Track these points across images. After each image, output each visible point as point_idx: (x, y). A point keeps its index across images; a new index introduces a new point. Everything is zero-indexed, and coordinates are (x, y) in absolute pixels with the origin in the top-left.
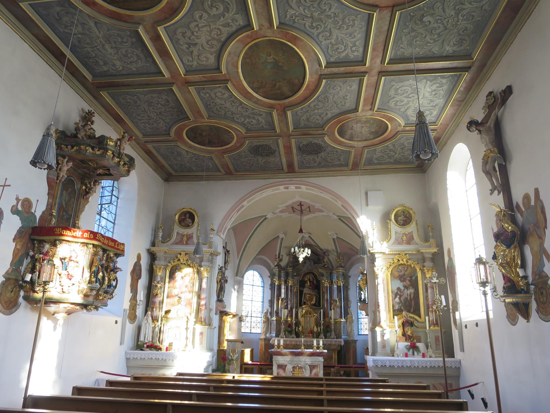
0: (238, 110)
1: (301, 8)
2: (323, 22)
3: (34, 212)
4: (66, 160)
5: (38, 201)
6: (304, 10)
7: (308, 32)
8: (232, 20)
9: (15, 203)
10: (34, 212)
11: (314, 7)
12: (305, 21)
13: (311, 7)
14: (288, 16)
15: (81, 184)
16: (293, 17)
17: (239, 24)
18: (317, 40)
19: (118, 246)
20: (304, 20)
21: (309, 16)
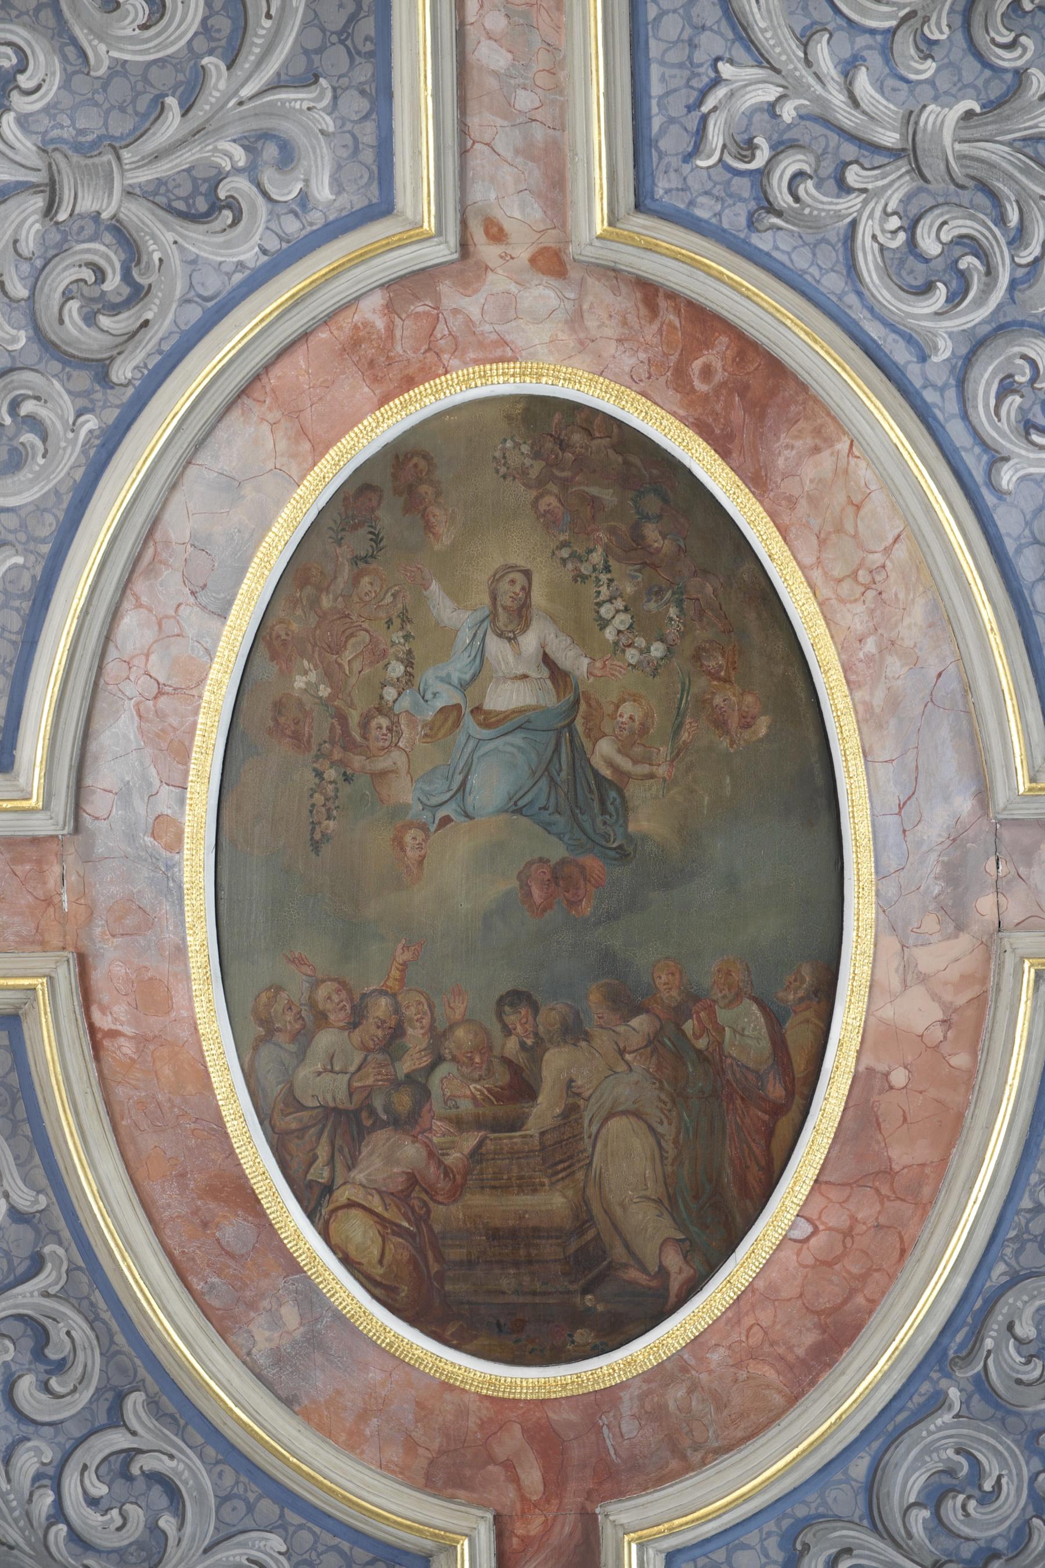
0: (59, 1513)
1: (822, 51)
2: (1001, 220)
6: (848, 68)
7: (874, 330)
8: (251, 144)
11: (927, 48)
12: (854, 201)
13: (905, 46)
14: (715, 136)
16: (751, 147)
17: (304, 199)
18: (957, 432)
20: (843, 188)
21: (890, 138)
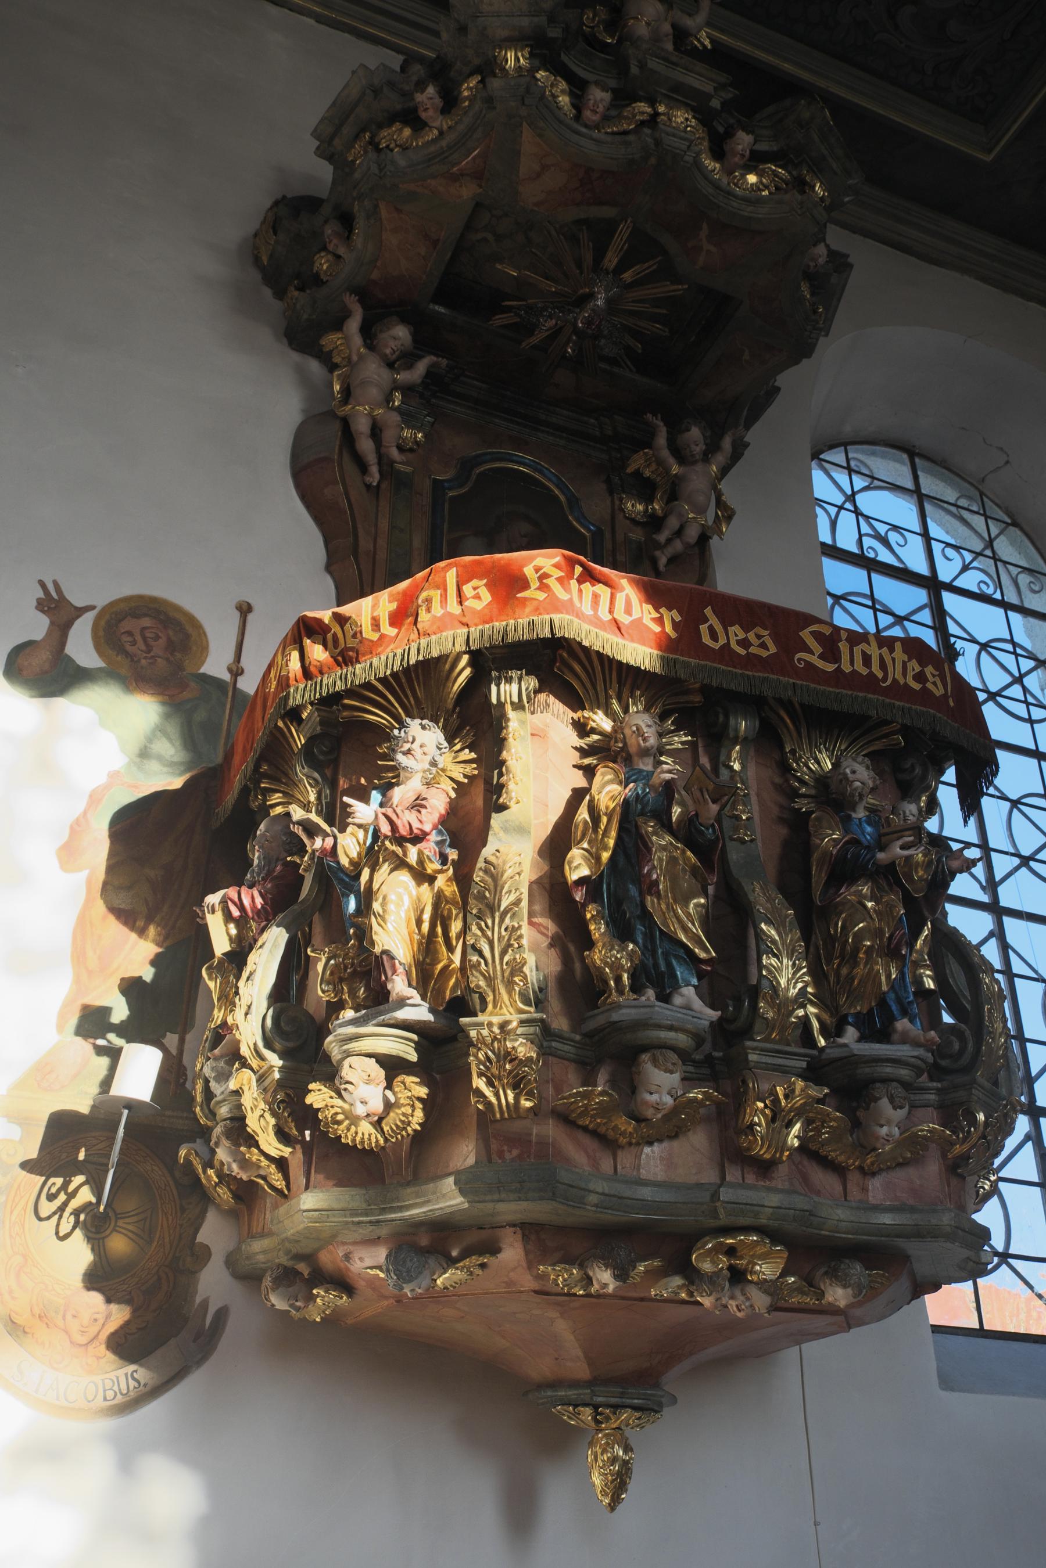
3: (226, 677)
4: (353, 325)
5: (245, 610)
9: (38, 626)
10: (226, 677)
15: (611, 492)
19: (831, 653)
